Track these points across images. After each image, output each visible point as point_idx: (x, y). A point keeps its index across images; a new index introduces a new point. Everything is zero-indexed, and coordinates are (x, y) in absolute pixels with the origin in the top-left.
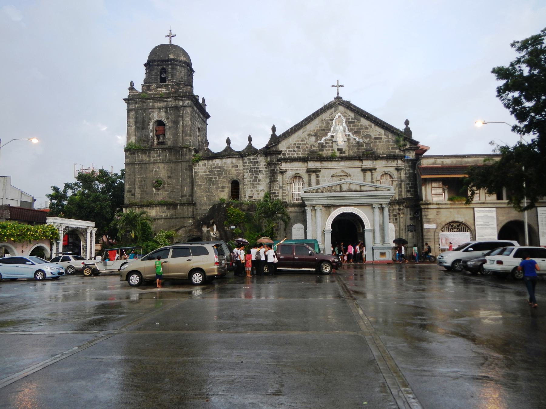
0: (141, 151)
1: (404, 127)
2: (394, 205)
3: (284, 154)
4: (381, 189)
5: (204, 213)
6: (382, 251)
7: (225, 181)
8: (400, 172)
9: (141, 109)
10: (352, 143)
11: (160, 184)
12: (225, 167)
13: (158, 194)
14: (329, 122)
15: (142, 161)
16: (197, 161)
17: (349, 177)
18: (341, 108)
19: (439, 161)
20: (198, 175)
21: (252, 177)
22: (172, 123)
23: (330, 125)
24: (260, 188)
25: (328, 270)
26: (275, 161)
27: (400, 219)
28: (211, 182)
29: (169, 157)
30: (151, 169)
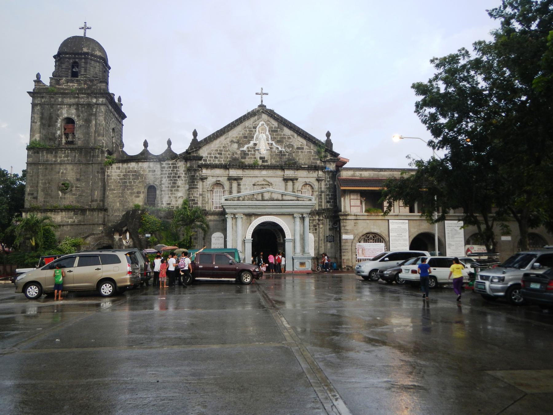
0: (46, 150)
1: (326, 138)
2: (314, 215)
3: (205, 160)
4: (302, 199)
5: (117, 220)
6: (302, 261)
7: (141, 186)
8: (321, 183)
9: (48, 104)
10: (275, 152)
11: (67, 187)
12: (141, 171)
13: (65, 198)
14: (252, 129)
15: (47, 161)
16: (111, 164)
17: (271, 187)
18: (264, 116)
19: (358, 173)
20: (111, 179)
21: (171, 183)
22: (83, 121)
23: (252, 133)
24: (178, 195)
25: (248, 280)
26: (195, 167)
27: (319, 229)
28: (126, 186)
29: (79, 157)
30: (57, 170)
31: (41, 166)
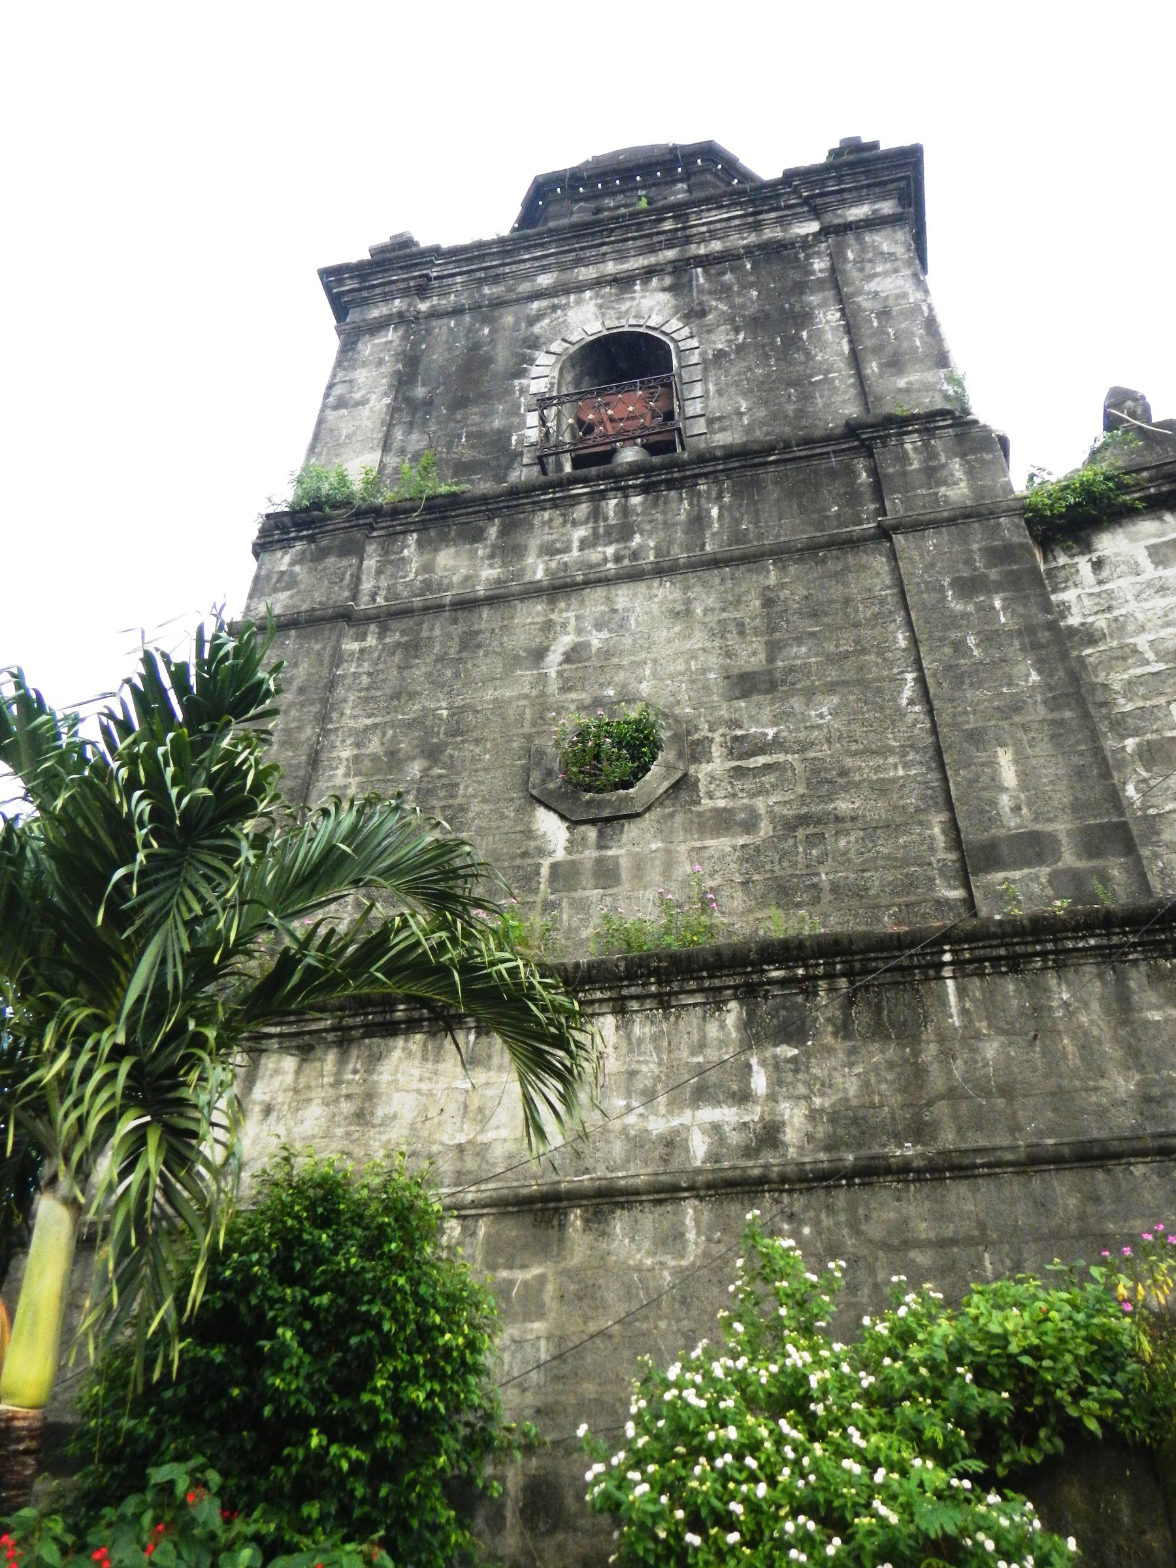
22: (737, 331)
31: (362, 637)
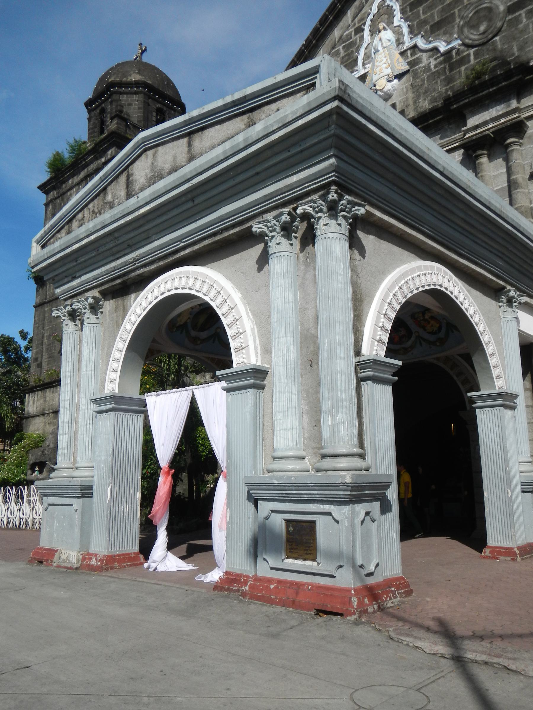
14: (354, 38)
